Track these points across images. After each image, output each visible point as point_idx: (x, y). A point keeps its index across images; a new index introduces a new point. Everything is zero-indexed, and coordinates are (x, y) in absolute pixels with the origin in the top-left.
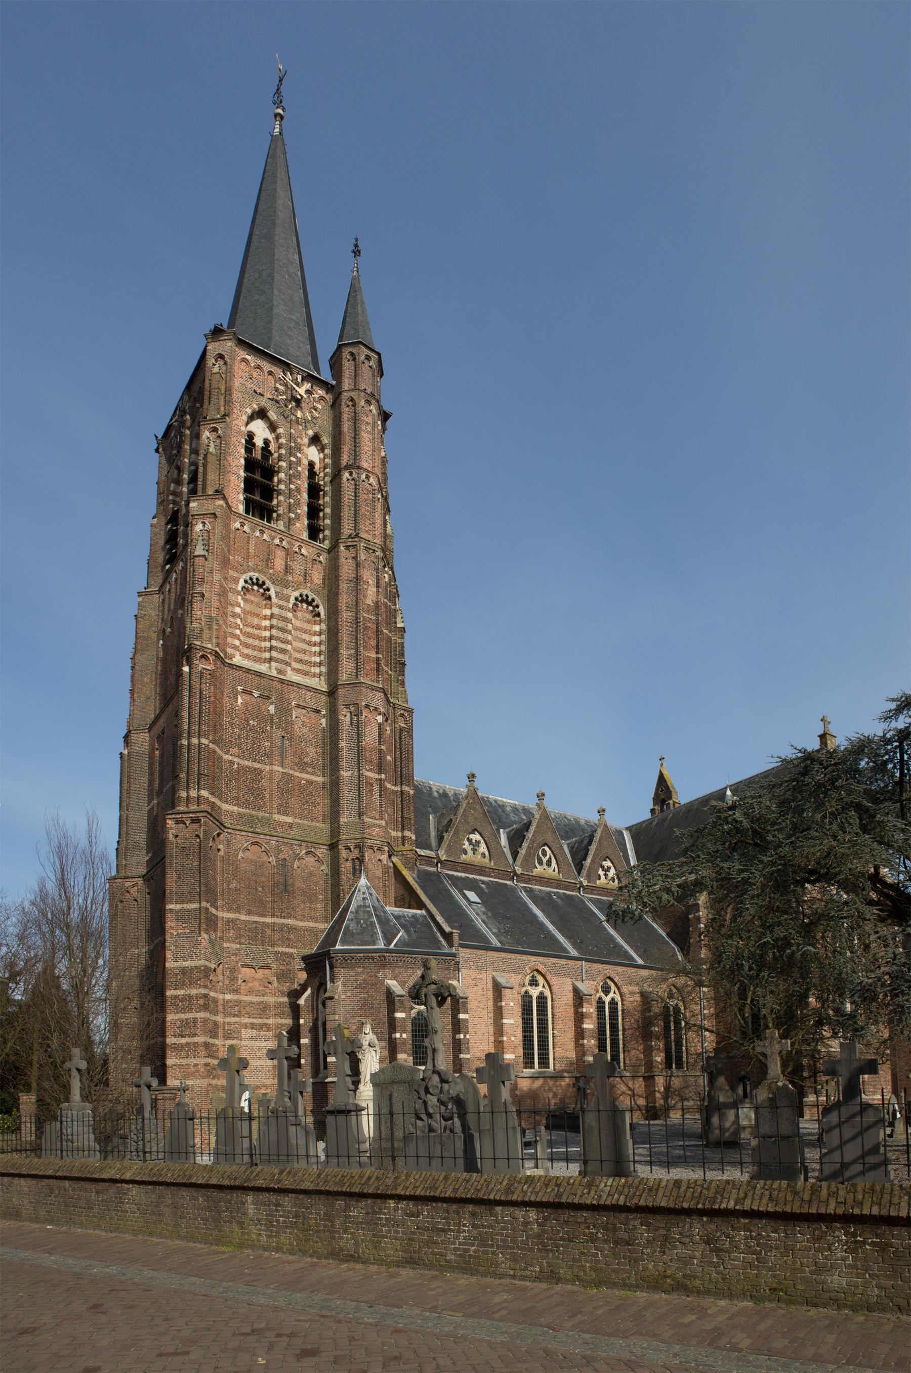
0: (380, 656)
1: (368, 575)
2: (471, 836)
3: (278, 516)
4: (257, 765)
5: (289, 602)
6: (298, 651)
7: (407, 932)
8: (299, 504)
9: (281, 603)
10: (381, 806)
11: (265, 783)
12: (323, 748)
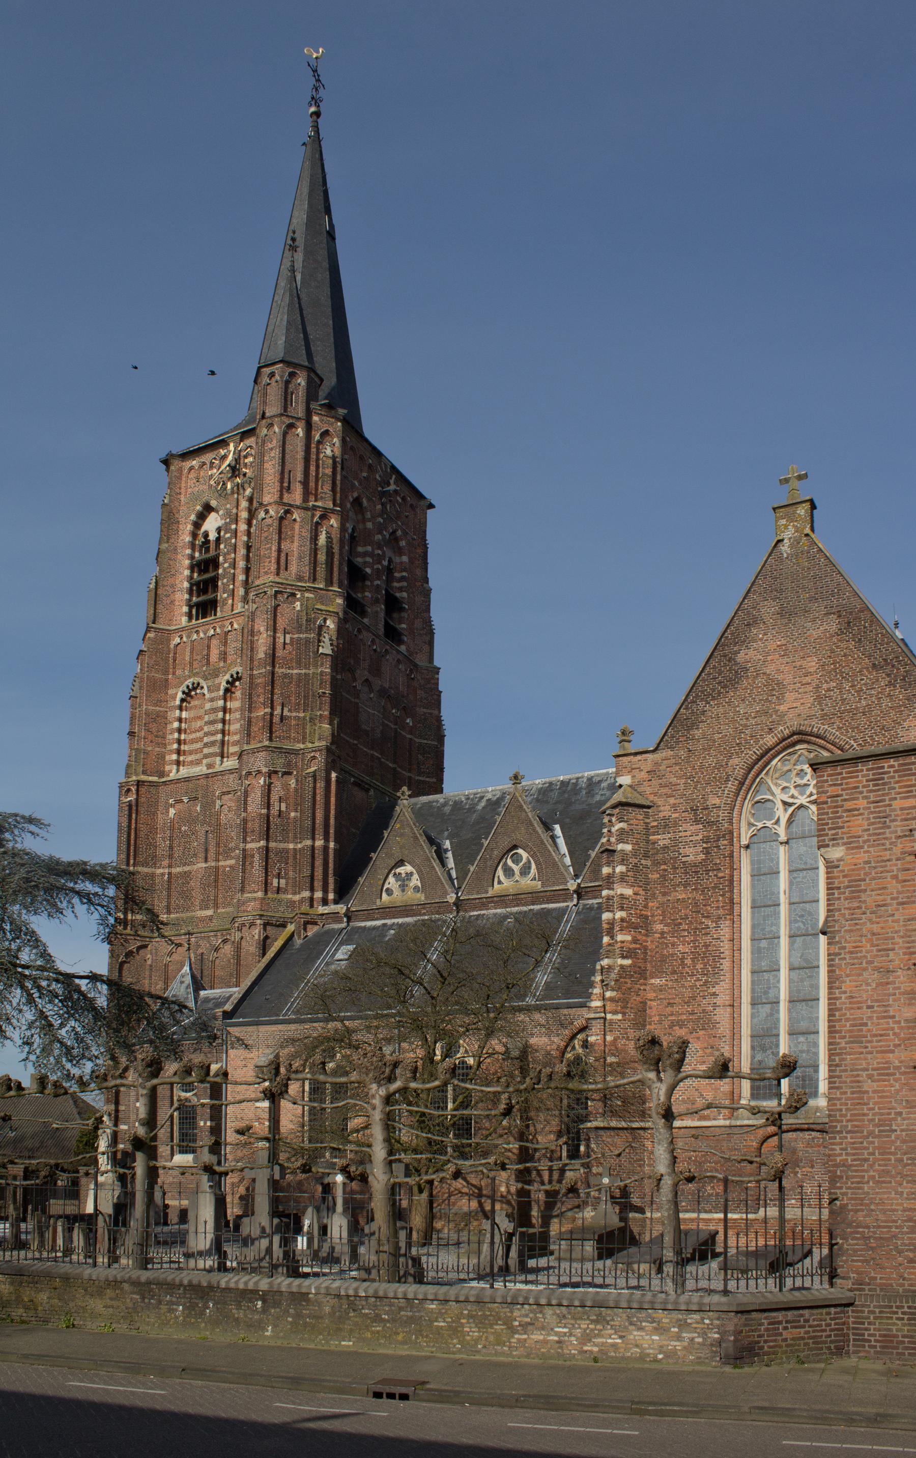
2: (398, 870)
4: (187, 868)
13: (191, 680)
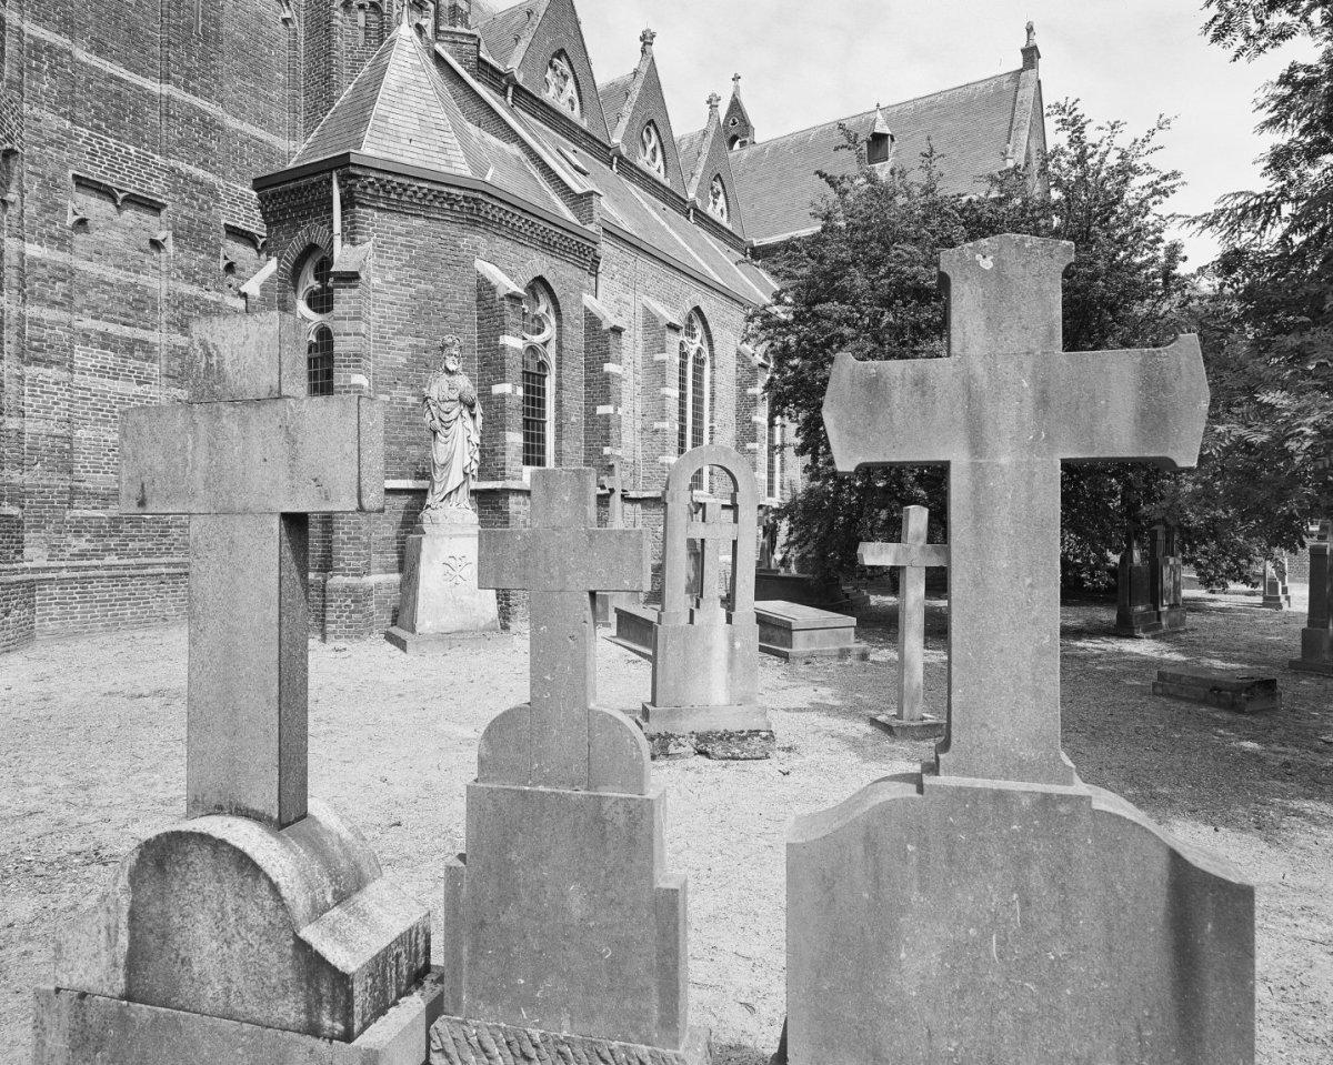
7: (498, 168)
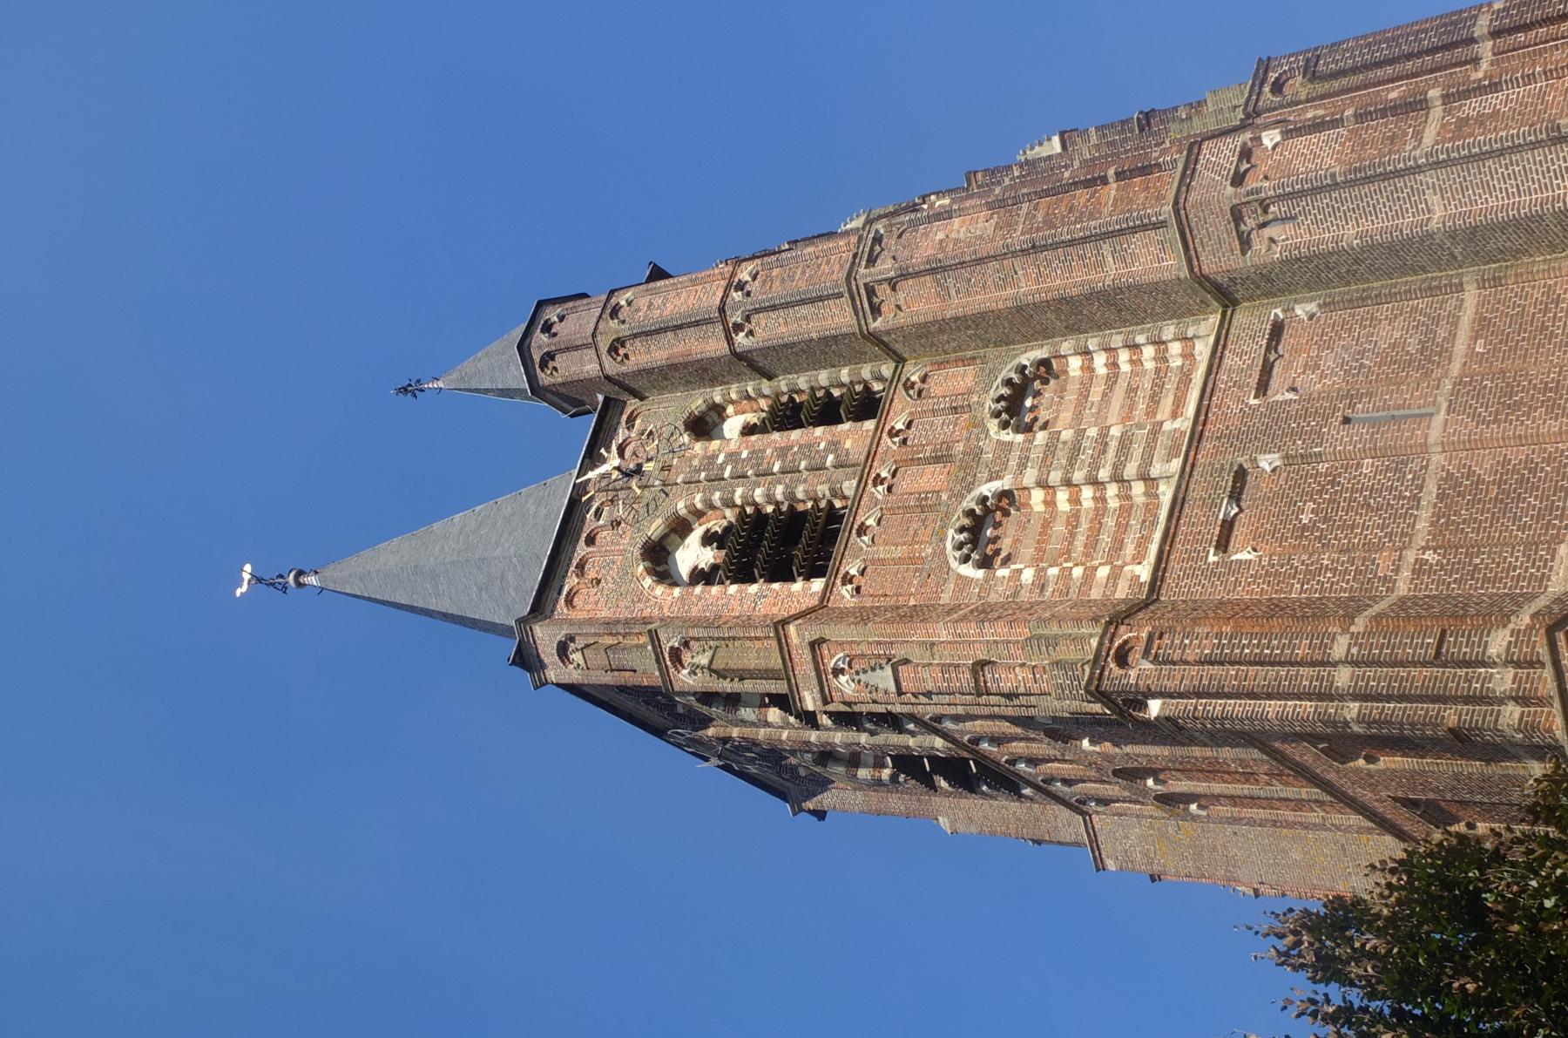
0: (1111, 172)
1: (930, 242)
3: (835, 495)
5: (1011, 444)
6: (1131, 408)
8: (809, 446)
9: (1013, 463)
10: (1530, 79)
11: (1484, 466)
12: (1378, 300)
13: (951, 532)
